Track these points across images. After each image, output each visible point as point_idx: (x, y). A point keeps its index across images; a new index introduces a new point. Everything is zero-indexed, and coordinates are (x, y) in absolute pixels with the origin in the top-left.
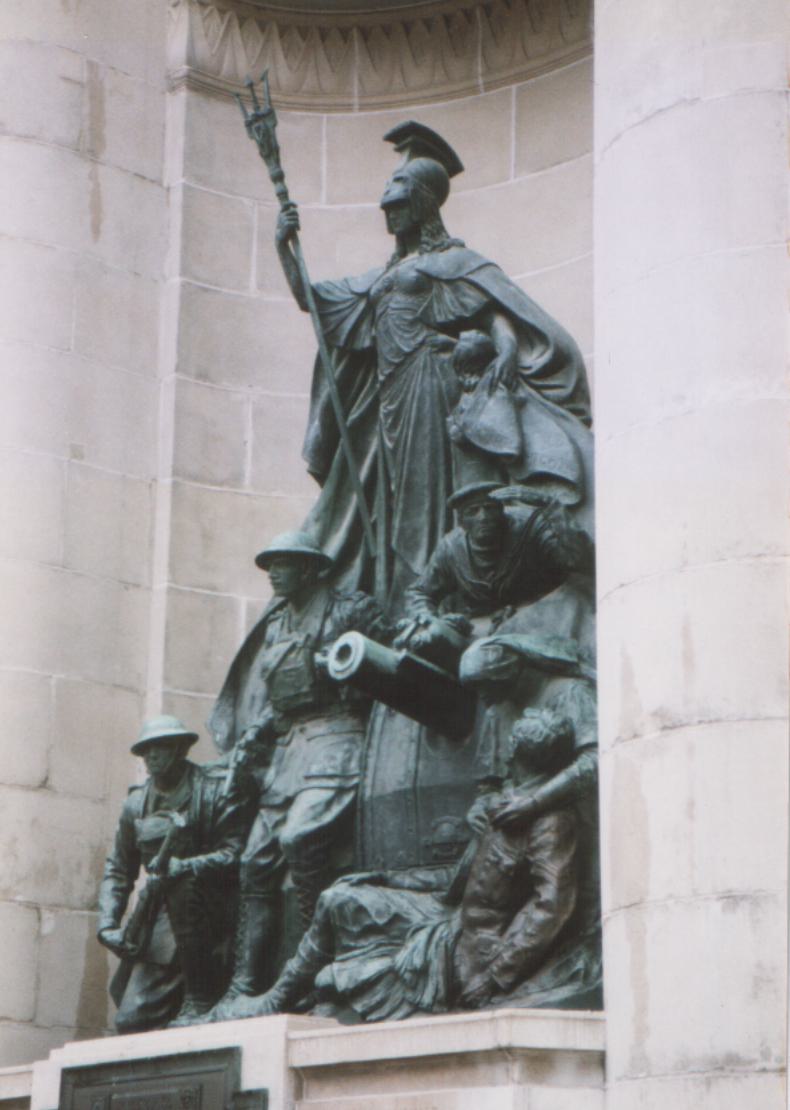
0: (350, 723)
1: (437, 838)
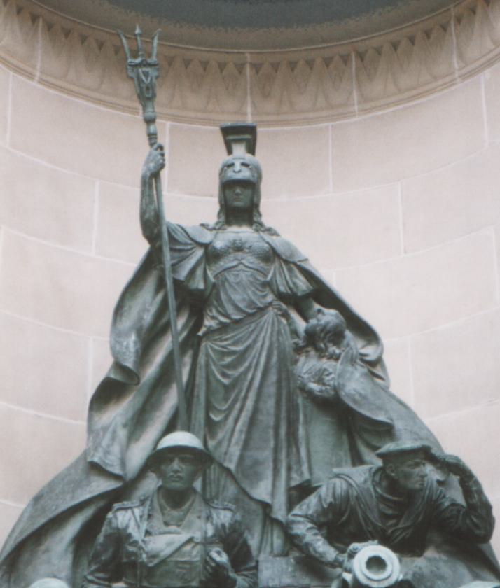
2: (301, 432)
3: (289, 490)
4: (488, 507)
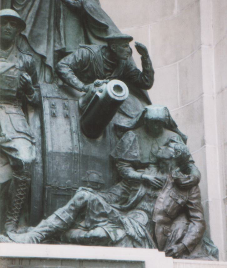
0: (21, 112)
1: (91, 179)
2: (61, 23)
3: (55, 51)
4: (153, 72)
